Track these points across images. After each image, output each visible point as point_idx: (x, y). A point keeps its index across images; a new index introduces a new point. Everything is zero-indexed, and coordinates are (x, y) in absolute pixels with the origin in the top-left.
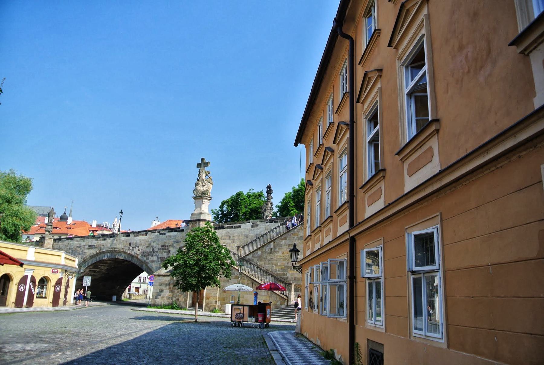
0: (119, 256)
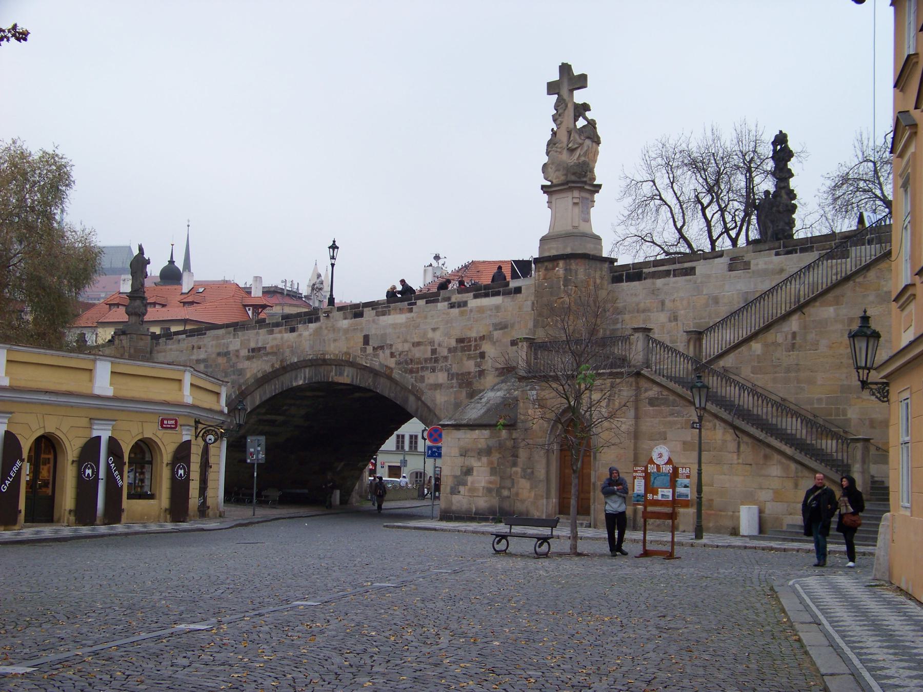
0: (336, 375)
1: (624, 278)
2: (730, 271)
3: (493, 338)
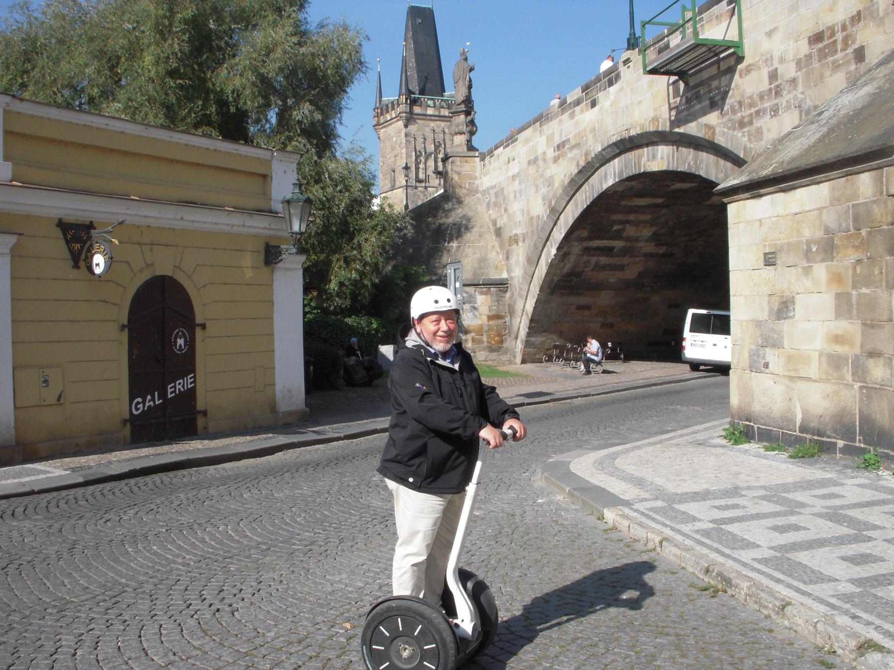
0: (648, 161)
3: (878, 9)
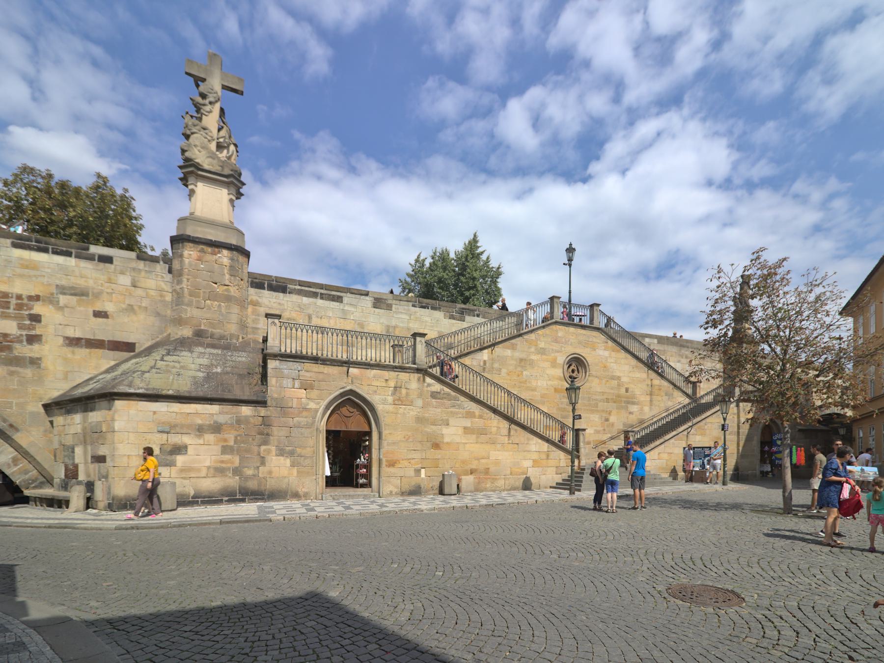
1: (266, 286)
2: (374, 307)
3: (58, 302)
